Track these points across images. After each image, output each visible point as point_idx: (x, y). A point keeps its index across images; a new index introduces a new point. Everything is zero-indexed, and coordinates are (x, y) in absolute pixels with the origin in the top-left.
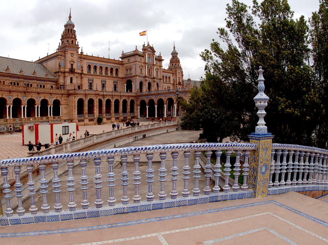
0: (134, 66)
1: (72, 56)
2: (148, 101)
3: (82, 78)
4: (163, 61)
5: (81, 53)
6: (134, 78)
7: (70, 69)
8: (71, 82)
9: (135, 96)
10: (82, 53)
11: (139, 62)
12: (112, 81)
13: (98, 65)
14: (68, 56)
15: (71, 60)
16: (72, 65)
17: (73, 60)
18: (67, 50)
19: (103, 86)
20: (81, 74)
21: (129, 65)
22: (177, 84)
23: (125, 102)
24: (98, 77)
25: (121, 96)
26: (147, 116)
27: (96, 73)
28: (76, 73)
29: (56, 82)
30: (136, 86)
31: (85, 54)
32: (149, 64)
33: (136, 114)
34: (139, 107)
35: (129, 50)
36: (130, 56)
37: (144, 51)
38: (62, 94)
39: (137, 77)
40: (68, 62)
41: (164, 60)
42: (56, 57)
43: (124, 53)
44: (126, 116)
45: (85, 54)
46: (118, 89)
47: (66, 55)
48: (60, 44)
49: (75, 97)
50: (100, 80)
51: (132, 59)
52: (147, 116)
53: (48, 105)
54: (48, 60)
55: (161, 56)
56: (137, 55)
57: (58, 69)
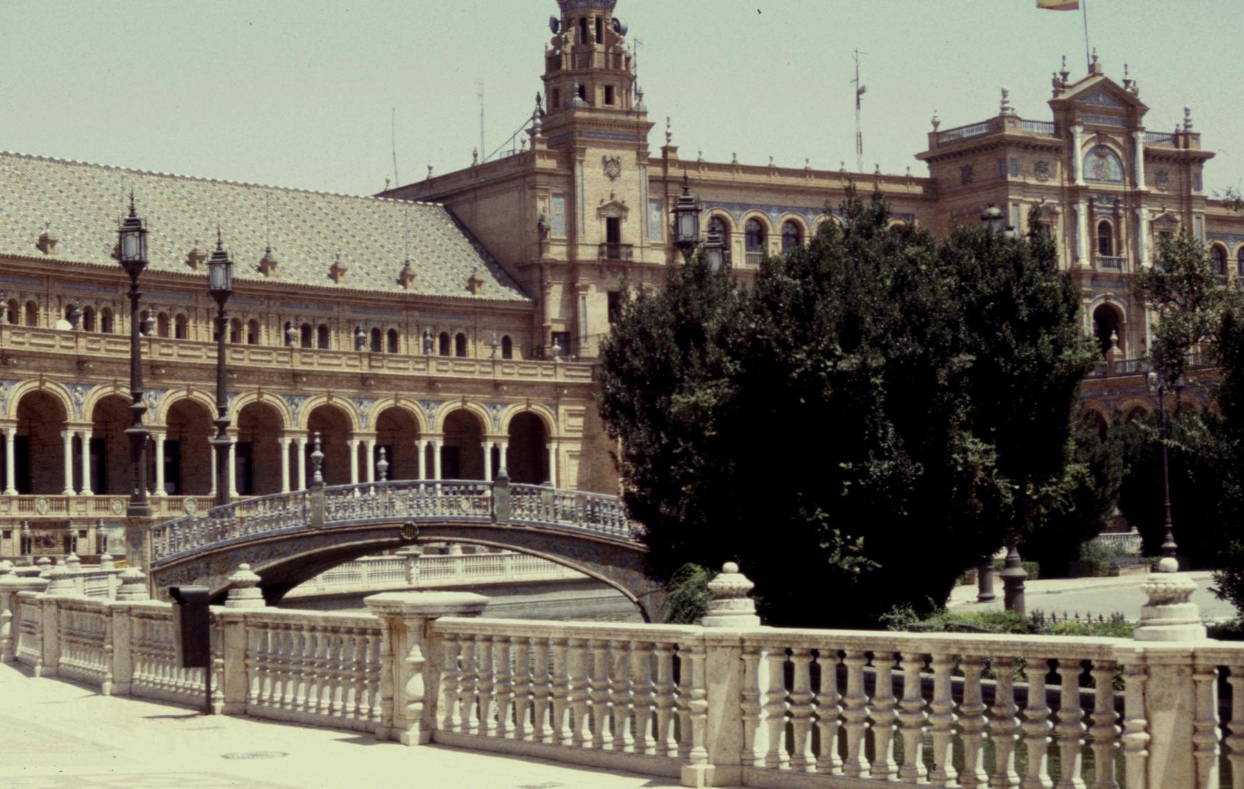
4: (1208, 164)
5: (665, 150)
7: (601, 246)
10: (670, 155)
11: (1024, 186)
15: (607, 202)
17: (618, 198)
31: (682, 155)
32: (1104, 194)
35: (967, 112)
37: (1062, 116)
41: (1210, 155)
43: (940, 129)
48: (539, 99)
53: (485, 439)
55: (1194, 130)
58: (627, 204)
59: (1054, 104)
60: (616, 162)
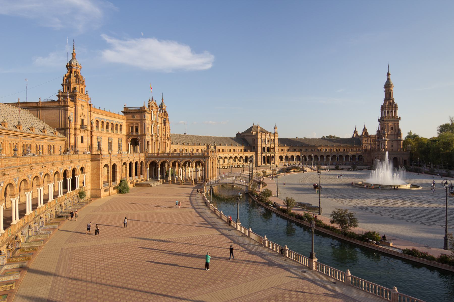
3: (92, 136)
8: (82, 142)
16: (82, 120)
19: (110, 145)
24: (105, 135)
59: (149, 106)
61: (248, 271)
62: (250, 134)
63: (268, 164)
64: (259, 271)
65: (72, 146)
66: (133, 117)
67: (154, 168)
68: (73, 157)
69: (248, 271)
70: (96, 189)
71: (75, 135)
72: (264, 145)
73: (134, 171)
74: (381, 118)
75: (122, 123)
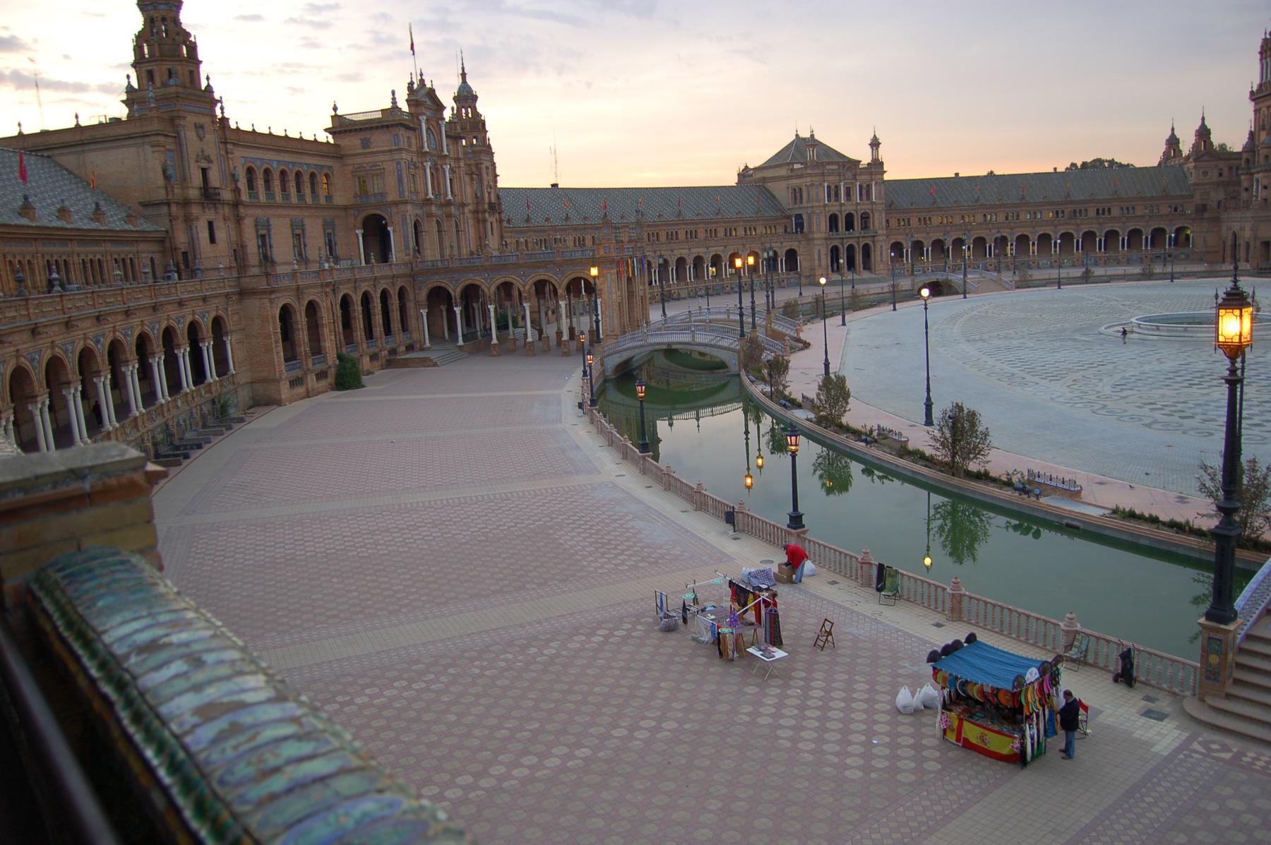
0: (390, 167)
1: (198, 136)
2: (459, 290)
3: (239, 220)
6: (394, 209)
8: (212, 240)
9: (410, 276)
12: (320, 221)
13: (275, 165)
14: (190, 135)
18: (181, 114)
20: (236, 204)
21: (369, 159)
22: (484, 211)
23: (385, 296)
24: (280, 211)
25: (376, 278)
26: (460, 338)
27: (274, 198)
28: (223, 203)
29: (164, 241)
30: (406, 237)
33: (415, 336)
34: (424, 312)
36: (372, 128)
38: (227, 295)
39: (409, 207)
40: (192, 161)
42: (140, 141)
43: (339, 113)
44: (393, 345)
45: (233, 126)
46: (339, 250)
47: (182, 134)
48: (128, 77)
49: (271, 301)
50: (287, 221)
51: (381, 141)
52: (460, 338)
54: (86, 148)
56: (402, 125)
57: (163, 191)
58: (213, 158)
60: (202, 127)
61: (623, 563)
62: (783, 172)
63: (849, 276)
64: (650, 563)
65: (185, 254)
66: (366, 143)
67: (443, 308)
68: (186, 289)
69: (623, 563)
70: (264, 381)
71: (188, 220)
72: (835, 209)
73: (378, 319)
74: (1260, 86)
75: (330, 167)
